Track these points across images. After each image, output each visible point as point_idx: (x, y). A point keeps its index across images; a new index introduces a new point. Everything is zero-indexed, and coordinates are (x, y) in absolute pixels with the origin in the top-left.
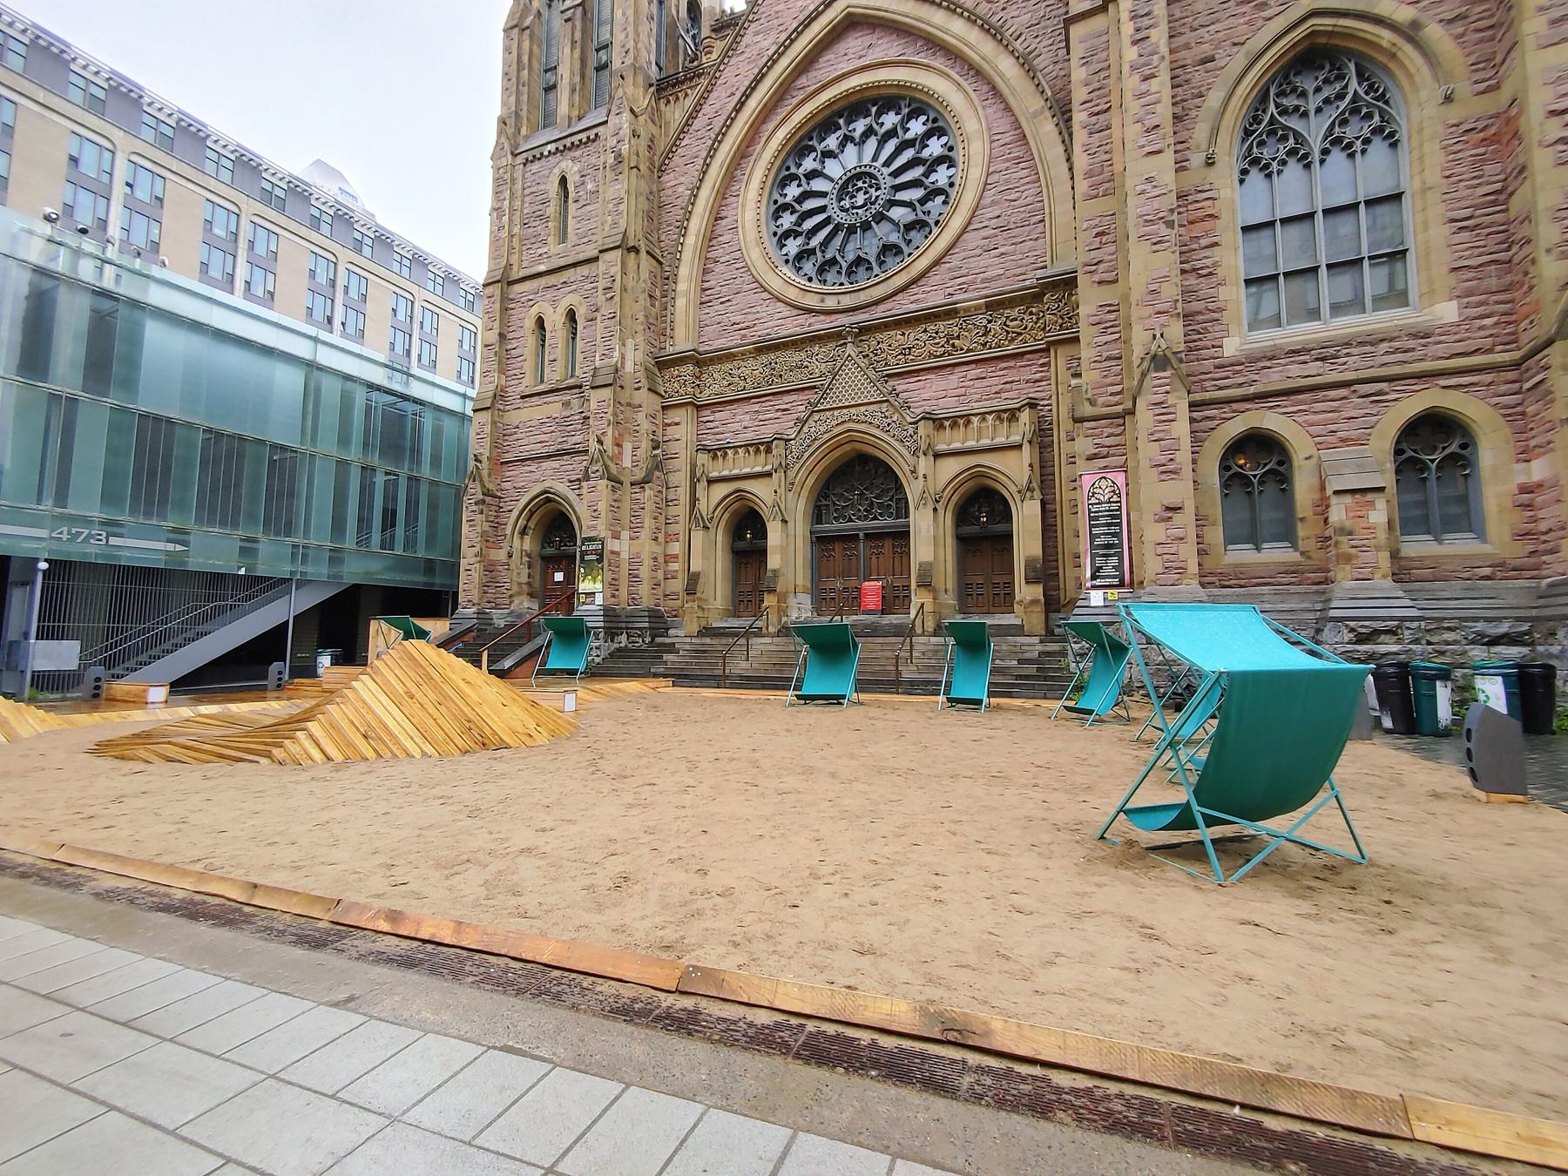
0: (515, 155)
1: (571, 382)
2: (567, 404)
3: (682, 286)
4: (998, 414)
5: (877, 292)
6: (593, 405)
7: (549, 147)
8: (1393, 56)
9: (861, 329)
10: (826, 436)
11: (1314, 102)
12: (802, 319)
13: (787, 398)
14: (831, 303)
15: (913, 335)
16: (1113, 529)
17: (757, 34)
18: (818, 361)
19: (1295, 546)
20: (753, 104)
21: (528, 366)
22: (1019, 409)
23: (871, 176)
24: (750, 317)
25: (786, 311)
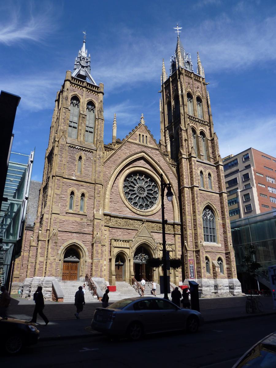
0: (67, 143)
1: (81, 213)
2: (82, 219)
3: (107, 196)
4: (169, 244)
5: (147, 214)
6: (95, 223)
7: (78, 147)
8: (214, 212)
9: (146, 221)
10: (140, 242)
11: (208, 213)
12: (133, 214)
13: (129, 230)
14: (138, 212)
15: (154, 224)
16: (193, 269)
17: (125, 148)
18: (137, 224)
19: (210, 274)
20: (124, 163)
21: (68, 204)
22: (172, 244)
23: (144, 188)
24: (121, 209)
25: (129, 211)
